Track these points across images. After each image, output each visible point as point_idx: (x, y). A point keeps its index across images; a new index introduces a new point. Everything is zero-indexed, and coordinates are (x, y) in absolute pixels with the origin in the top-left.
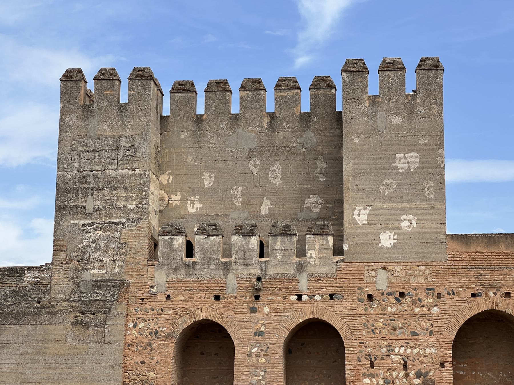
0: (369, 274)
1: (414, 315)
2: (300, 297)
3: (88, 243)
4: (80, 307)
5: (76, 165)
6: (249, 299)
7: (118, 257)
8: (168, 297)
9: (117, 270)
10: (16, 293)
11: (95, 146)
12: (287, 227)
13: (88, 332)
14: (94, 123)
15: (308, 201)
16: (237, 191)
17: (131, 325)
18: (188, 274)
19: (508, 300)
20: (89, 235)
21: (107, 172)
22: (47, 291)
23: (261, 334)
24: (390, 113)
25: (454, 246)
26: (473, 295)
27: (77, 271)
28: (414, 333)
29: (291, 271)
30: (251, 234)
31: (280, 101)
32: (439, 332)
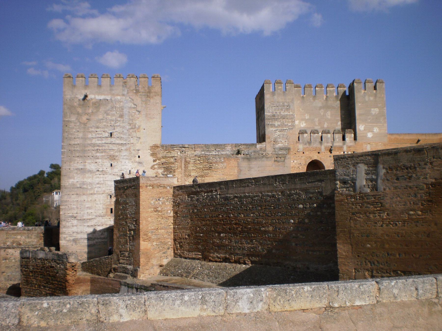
0: (365, 146)
3: (276, 136)
4: (276, 156)
5: (271, 111)
7: (287, 140)
8: (303, 153)
9: (286, 144)
10: (255, 152)
11: (277, 105)
14: (276, 97)
16: (317, 120)
20: (277, 133)
21: (281, 113)
22: (265, 151)
27: (274, 144)
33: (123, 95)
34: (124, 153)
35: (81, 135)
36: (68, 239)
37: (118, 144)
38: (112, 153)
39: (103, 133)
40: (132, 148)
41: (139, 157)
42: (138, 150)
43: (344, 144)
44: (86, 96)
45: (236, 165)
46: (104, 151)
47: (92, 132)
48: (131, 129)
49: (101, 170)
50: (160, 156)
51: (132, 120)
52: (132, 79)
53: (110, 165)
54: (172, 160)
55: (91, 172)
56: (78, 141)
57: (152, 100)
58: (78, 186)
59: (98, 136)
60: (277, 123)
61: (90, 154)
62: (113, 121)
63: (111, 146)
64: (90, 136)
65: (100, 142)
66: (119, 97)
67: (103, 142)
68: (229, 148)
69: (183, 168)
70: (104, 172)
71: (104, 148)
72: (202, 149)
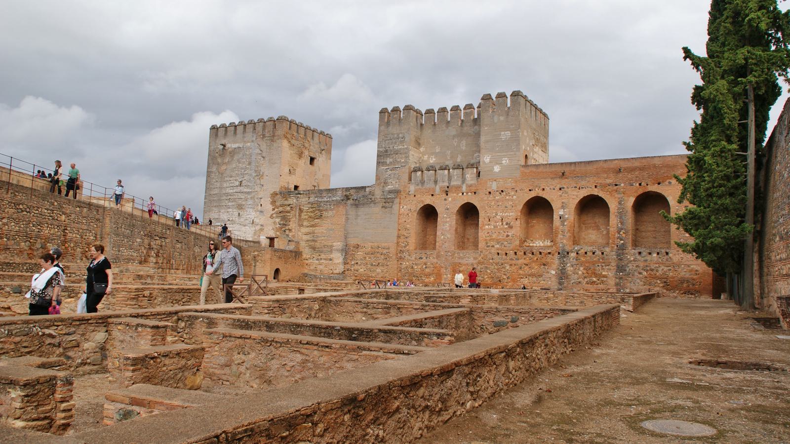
0: (489, 183)
2: (463, 193)
4: (384, 201)
6: (444, 195)
10: (363, 196)
12: (459, 165)
13: (386, 210)
14: (390, 128)
15: (475, 155)
16: (449, 152)
17: (401, 207)
18: (422, 186)
19: (544, 192)
22: (373, 195)
23: (448, 209)
24: (499, 115)
25: (523, 169)
26: (530, 190)
27: (383, 187)
28: (506, 207)
29: (459, 183)
31: (466, 114)
32: (516, 206)
33: (253, 141)
34: (250, 202)
35: (218, 185)
38: (240, 202)
39: (235, 182)
40: (256, 196)
44: (224, 146)
45: (345, 213)
46: (234, 200)
47: (227, 181)
49: (230, 219)
50: (278, 204)
51: (257, 167)
52: (260, 123)
53: (238, 214)
54: (288, 208)
56: (216, 191)
57: (275, 145)
60: (388, 161)
61: (224, 204)
62: (243, 169)
63: (239, 194)
64: (225, 185)
65: (232, 191)
66: (249, 144)
67: (234, 191)
68: (339, 193)
69: (297, 217)
70: (233, 222)
71: (234, 197)
72: (315, 195)
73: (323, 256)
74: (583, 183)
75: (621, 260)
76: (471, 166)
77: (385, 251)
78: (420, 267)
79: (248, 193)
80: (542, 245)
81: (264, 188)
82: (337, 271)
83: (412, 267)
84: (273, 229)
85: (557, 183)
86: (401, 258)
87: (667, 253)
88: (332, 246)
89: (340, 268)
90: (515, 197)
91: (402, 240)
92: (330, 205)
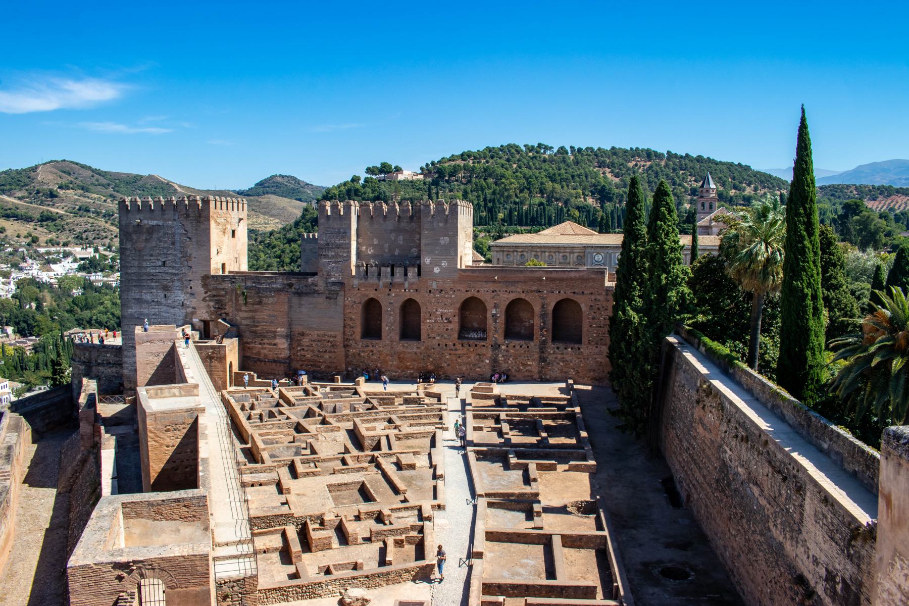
1: (445, 297)
4: (327, 292)
6: (387, 290)
10: (306, 286)
13: (332, 301)
14: (331, 222)
23: (391, 303)
30: (388, 266)
33: (175, 220)
35: (136, 263)
36: (130, 368)
37: (171, 273)
40: (184, 278)
41: (191, 288)
42: (190, 281)
43: (406, 280)
46: (157, 281)
48: (183, 257)
50: (211, 287)
53: (163, 296)
54: (223, 292)
55: (147, 302)
56: (133, 270)
58: (136, 316)
59: (152, 264)
60: (331, 254)
61: (145, 284)
63: (164, 275)
64: (145, 264)
65: (153, 271)
67: (157, 271)
69: (234, 301)
70: (159, 303)
73: (266, 341)
74: (513, 288)
75: (543, 352)
76: (413, 266)
77: (331, 339)
78: (366, 354)
79: (174, 274)
80: (476, 336)
81: (194, 270)
82: (283, 356)
83: (359, 354)
84: (207, 312)
85: (491, 287)
86: (347, 346)
87: (579, 349)
88: (275, 332)
89: (285, 354)
90: (453, 296)
91: (347, 330)
92: (270, 291)
